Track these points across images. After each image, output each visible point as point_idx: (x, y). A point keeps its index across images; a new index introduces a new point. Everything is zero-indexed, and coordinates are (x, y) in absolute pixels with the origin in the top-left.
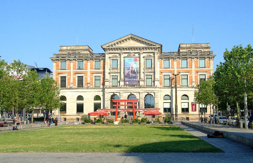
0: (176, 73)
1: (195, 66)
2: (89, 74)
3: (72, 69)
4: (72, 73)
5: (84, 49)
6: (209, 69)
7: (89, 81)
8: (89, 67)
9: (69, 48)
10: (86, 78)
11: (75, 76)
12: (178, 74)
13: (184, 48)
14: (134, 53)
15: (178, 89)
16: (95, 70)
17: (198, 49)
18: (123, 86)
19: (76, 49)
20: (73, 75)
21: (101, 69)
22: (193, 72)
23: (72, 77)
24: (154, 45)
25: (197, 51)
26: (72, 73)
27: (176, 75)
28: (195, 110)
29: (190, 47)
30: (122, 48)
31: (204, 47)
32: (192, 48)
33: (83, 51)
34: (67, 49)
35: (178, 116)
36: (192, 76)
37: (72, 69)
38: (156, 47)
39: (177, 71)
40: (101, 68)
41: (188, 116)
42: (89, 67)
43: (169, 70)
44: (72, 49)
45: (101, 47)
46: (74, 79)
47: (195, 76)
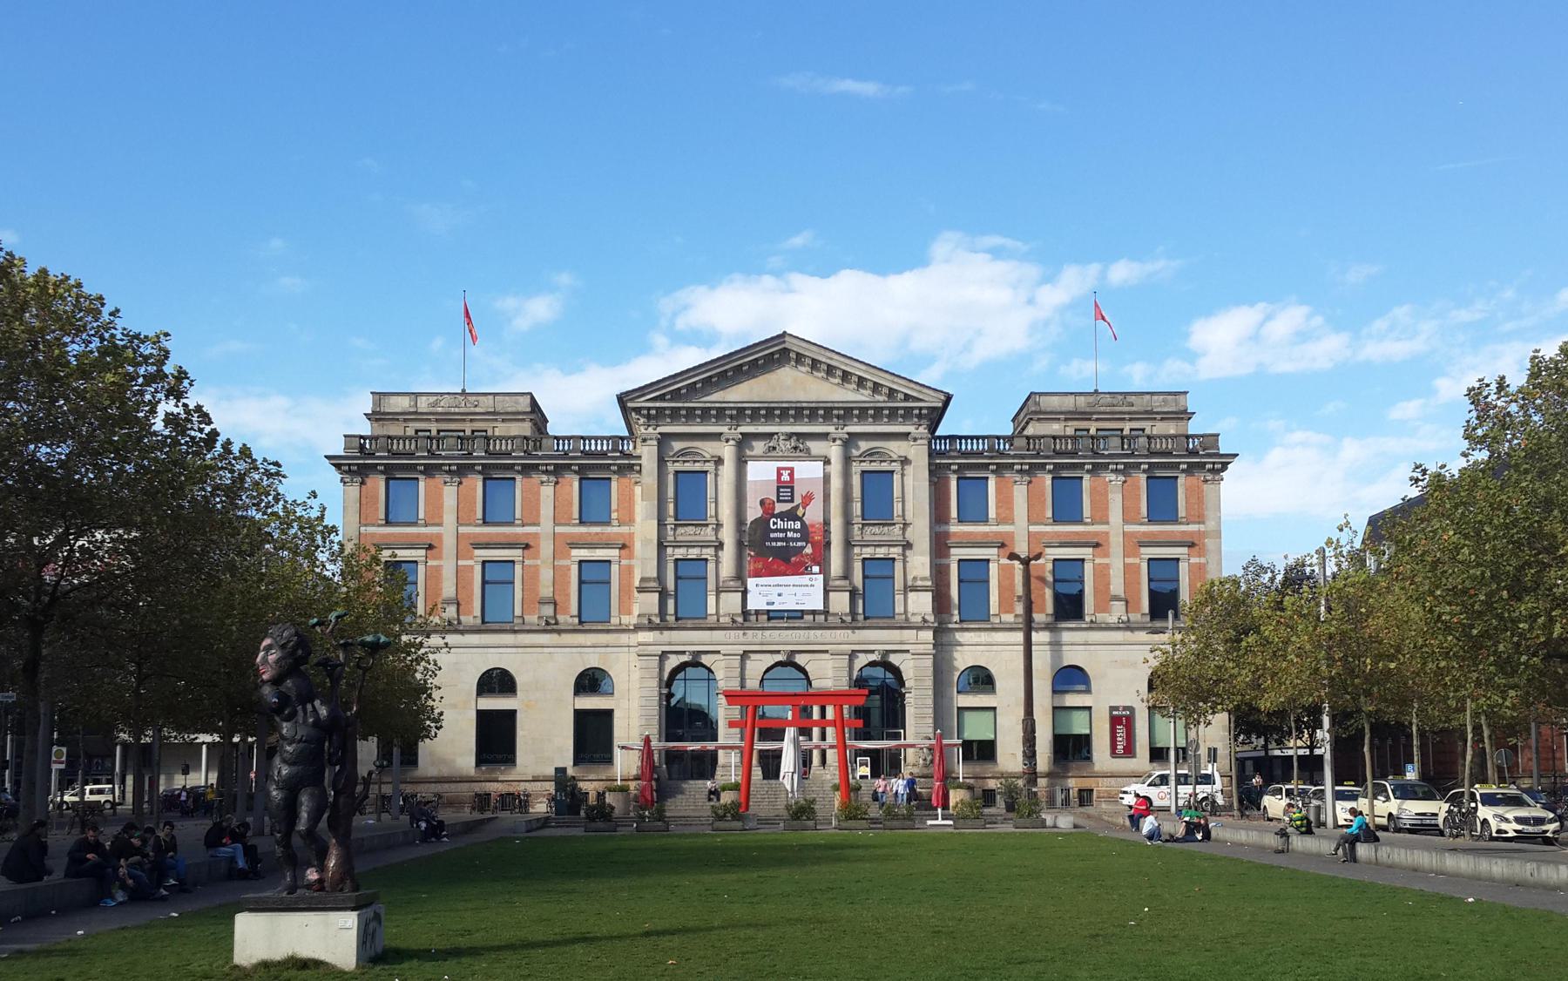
2: (546, 549)
4: (449, 543)
5: (509, 410)
6: (1202, 527)
7: (546, 591)
8: (546, 511)
10: (531, 577)
12: (1038, 557)
14: (800, 436)
16: (583, 529)
17: (1131, 420)
19: (462, 410)
21: (615, 523)
22: (1116, 543)
23: (447, 565)
24: (907, 397)
25: (1122, 430)
26: (449, 543)
28: (1129, 751)
29: (1088, 410)
30: (731, 408)
31: (1158, 413)
32: (1095, 417)
33: (503, 420)
34: (412, 410)
36: (1107, 566)
37: (449, 518)
40: (614, 515)
42: (546, 511)
43: (986, 534)
44: (440, 410)
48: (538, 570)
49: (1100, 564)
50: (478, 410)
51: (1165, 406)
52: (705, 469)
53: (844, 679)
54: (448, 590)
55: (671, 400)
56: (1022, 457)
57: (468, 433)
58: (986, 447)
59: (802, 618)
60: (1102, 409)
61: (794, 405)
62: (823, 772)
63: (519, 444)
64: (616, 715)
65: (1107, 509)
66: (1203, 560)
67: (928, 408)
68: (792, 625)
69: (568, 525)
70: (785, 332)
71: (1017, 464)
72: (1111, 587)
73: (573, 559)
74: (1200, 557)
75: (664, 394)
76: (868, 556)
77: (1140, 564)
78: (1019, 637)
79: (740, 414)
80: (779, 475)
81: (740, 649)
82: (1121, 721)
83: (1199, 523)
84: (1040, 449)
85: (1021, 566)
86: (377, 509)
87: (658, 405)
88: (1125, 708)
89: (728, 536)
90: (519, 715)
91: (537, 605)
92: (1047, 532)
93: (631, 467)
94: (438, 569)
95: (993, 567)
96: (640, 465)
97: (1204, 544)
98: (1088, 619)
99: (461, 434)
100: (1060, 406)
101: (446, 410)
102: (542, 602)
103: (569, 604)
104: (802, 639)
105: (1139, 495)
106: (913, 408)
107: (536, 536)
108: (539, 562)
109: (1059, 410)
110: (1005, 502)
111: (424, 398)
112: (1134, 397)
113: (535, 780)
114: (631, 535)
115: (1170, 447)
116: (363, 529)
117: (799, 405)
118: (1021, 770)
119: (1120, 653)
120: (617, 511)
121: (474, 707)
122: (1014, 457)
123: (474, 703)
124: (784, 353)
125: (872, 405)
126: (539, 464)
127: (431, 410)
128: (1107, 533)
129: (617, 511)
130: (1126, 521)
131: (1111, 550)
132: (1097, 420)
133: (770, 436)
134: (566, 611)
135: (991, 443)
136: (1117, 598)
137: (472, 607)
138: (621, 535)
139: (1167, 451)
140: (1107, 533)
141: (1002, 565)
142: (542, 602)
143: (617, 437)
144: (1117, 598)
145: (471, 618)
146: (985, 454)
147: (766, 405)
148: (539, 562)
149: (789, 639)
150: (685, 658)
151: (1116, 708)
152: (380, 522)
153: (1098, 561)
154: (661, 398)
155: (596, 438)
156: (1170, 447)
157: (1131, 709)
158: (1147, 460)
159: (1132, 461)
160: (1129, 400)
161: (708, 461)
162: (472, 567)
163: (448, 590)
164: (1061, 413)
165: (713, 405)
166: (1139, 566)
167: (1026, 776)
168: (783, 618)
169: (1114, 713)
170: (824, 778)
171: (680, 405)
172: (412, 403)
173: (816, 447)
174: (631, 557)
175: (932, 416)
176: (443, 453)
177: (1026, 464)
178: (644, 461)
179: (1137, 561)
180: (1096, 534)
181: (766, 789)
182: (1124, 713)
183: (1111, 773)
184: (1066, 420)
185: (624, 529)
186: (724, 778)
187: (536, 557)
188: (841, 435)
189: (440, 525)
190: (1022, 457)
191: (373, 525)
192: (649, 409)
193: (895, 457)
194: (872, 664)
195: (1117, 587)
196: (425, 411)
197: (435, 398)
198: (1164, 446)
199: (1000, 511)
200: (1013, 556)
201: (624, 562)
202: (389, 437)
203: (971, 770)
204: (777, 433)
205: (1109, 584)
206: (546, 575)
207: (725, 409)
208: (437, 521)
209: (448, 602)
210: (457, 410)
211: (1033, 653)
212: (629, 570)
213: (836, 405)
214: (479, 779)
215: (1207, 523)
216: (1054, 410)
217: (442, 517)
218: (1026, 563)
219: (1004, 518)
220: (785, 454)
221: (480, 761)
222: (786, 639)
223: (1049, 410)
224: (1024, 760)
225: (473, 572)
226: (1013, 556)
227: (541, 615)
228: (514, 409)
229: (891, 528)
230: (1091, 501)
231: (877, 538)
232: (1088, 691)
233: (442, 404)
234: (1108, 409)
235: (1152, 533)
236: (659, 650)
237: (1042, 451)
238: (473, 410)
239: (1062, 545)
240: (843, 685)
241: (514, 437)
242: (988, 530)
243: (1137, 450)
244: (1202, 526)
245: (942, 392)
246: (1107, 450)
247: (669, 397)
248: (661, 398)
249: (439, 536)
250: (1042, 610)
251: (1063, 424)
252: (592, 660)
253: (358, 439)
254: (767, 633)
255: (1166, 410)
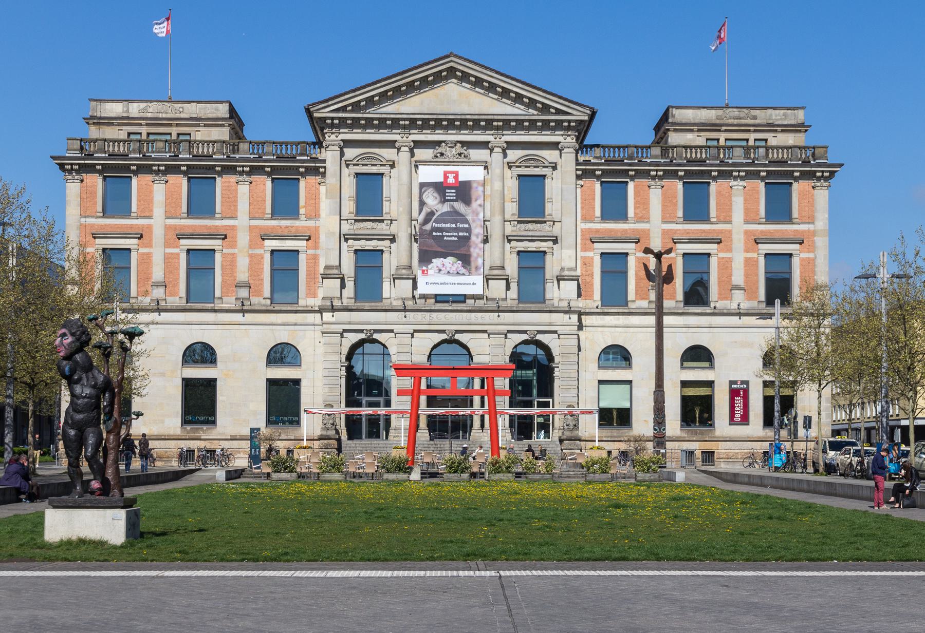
0: (657, 246)
1: (747, 211)
2: (243, 239)
3: (158, 211)
4: (158, 233)
5: (210, 116)
6: (811, 227)
7: (242, 275)
8: (243, 206)
9: (135, 109)
10: (231, 262)
11: (176, 250)
12: (669, 251)
13: (686, 127)
14: (463, 143)
15: (667, 320)
17: (755, 131)
18: (408, 299)
19: (169, 116)
20: (167, 244)
21: (303, 217)
23: (158, 253)
24: (559, 112)
25: (747, 140)
26: (158, 233)
27: (658, 256)
28: (745, 419)
29: (718, 122)
30: (404, 119)
31: (779, 126)
32: (724, 128)
33: (205, 125)
34: (125, 115)
35: (669, 445)
36: (730, 260)
37: (158, 211)
38: (569, 121)
39: (665, 232)
41: (708, 446)
42: (243, 206)
43: (625, 231)
44: (149, 115)
45: (308, 111)
46: (169, 260)
47: (748, 261)
48: (236, 258)
49: (723, 258)
50: (182, 116)
51: (785, 119)
52: (381, 172)
53: (500, 355)
54: (158, 273)
55: (352, 111)
56: (658, 164)
57: (174, 137)
58: (626, 155)
59: (465, 302)
60: (731, 121)
61: (459, 117)
62: (481, 434)
63: (219, 148)
64: (304, 384)
65: (730, 210)
66: (811, 255)
67: (576, 121)
68: (455, 308)
69: (262, 219)
70: (451, 53)
71: (653, 170)
72: (733, 278)
73: (266, 248)
74: (809, 252)
75: (346, 106)
76: (522, 249)
77: (757, 258)
78: (652, 320)
79: (413, 123)
80: (446, 177)
81: (410, 328)
82: (738, 392)
83: (809, 223)
84: (673, 157)
85: (655, 259)
86: (96, 203)
87: (340, 115)
88: (743, 382)
89: (402, 231)
90: (219, 383)
91: (235, 289)
92: (677, 230)
93: (317, 168)
94: (148, 256)
95: (631, 261)
96: (325, 167)
97: (814, 242)
98: (712, 305)
99: (168, 137)
100: (694, 119)
101: (155, 115)
102: (239, 286)
103: (262, 288)
104: (465, 320)
105: (758, 198)
106: (563, 121)
107: (234, 228)
108: (236, 251)
109: (692, 121)
110: (643, 203)
111: (135, 105)
112: (758, 111)
113: (233, 439)
114: (317, 229)
115: (785, 156)
116: (83, 220)
117: (463, 117)
118: (652, 435)
119: (740, 335)
120: (305, 207)
121: (180, 376)
122: (650, 164)
123: (179, 372)
124: (451, 71)
125: (527, 118)
126: (236, 166)
127: (142, 115)
128: (730, 231)
129: (305, 207)
130: (747, 222)
131: (733, 246)
132: (726, 131)
133: (439, 143)
134: (259, 293)
135: (630, 152)
136: (738, 288)
137: (179, 289)
138: (309, 228)
139: (783, 160)
140: (730, 231)
141: (637, 257)
142: (239, 286)
143: (304, 142)
144: (738, 288)
145: (177, 299)
146: (625, 161)
147: (435, 117)
148: (236, 251)
149: (453, 320)
150: (362, 336)
151: (735, 382)
152: (99, 214)
153: (721, 255)
154: (343, 109)
155: (287, 144)
156: (785, 156)
157: (747, 383)
158: (765, 169)
159: (752, 169)
160: (753, 114)
161: (384, 165)
162: (178, 254)
163: (158, 273)
164: (694, 125)
165: (388, 116)
166: (757, 261)
167: (656, 440)
168: (448, 302)
169: (734, 386)
170: (482, 440)
171: (360, 115)
172: (125, 109)
173: (475, 154)
174: (316, 247)
175: (579, 128)
176: (153, 155)
177: (660, 170)
178: (328, 165)
179: (755, 255)
180: (721, 232)
181: (432, 449)
182: (742, 386)
183: (729, 437)
184: (699, 130)
185: (311, 223)
186: (395, 439)
187: (234, 246)
188: (500, 144)
189: (150, 217)
190: (658, 164)
191: (92, 217)
192: (332, 119)
193: (547, 164)
194: (525, 342)
195: (738, 278)
196: (136, 116)
197: (145, 104)
198: (780, 156)
199: (638, 211)
200: (647, 251)
201: (310, 252)
202: (105, 140)
203: (609, 434)
204: (444, 141)
205: (731, 275)
206: (243, 263)
207: (399, 119)
208: (147, 214)
209: (157, 284)
210: (164, 116)
211: (665, 335)
212: (314, 259)
213: (496, 117)
214: (183, 438)
215: (816, 223)
216: (688, 121)
217: (152, 210)
218: (658, 256)
219: (640, 218)
220: (451, 160)
221: (185, 422)
222: (451, 320)
223: (684, 121)
224: (654, 426)
225: (179, 259)
226: (647, 251)
227: (239, 297)
228: (214, 116)
229: (543, 225)
230: (717, 203)
231: (530, 234)
232: (712, 367)
233: (151, 110)
234: (736, 122)
235: (769, 232)
236: (340, 328)
237: (675, 160)
238: (177, 116)
239: (691, 241)
240: (503, 359)
241: (215, 142)
242: (627, 228)
243: (757, 159)
244: (812, 226)
245: (588, 107)
246: (732, 159)
247: (350, 108)
248: (343, 109)
249: (150, 227)
250: (673, 297)
251: (697, 134)
252: (283, 336)
253: (79, 141)
254: (434, 314)
255: (786, 122)
